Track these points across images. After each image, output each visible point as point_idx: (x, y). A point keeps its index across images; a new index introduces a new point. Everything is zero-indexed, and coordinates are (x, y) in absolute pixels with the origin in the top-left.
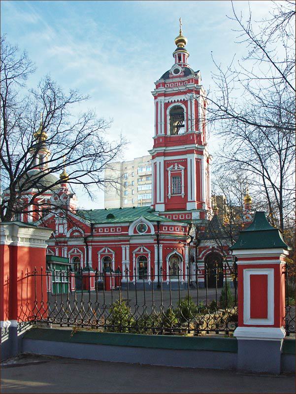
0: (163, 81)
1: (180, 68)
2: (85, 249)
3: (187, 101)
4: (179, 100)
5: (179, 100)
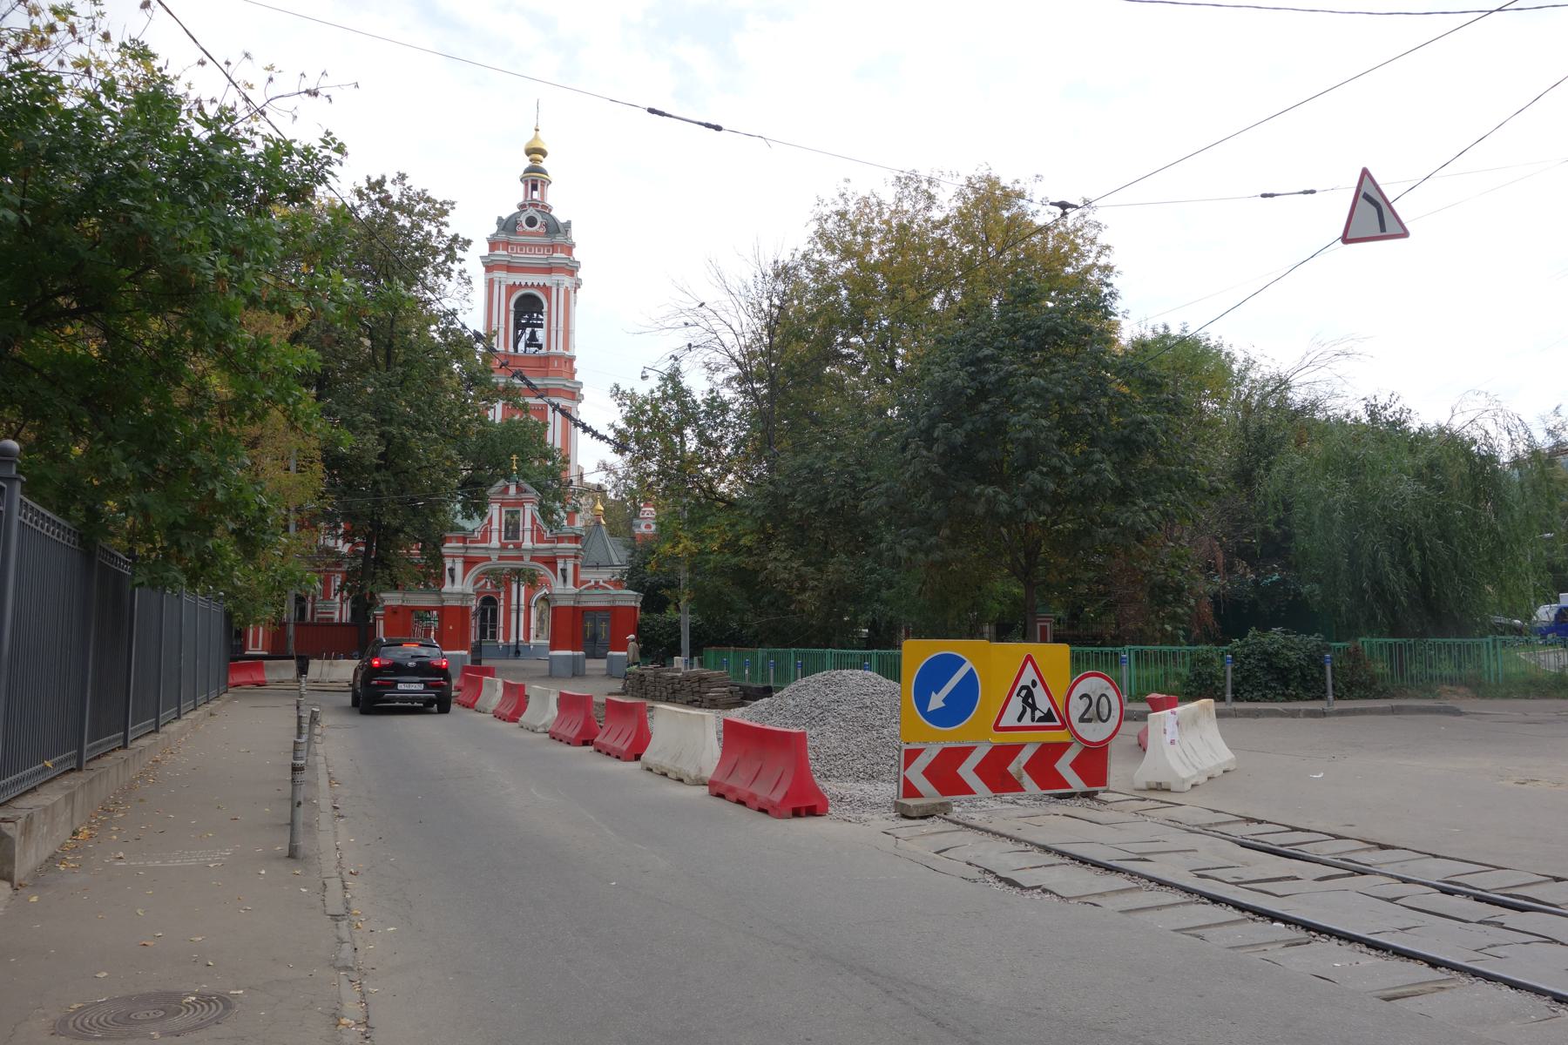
0: (503, 236)
1: (539, 219)
4: (536, 284)
5: (536, 284)
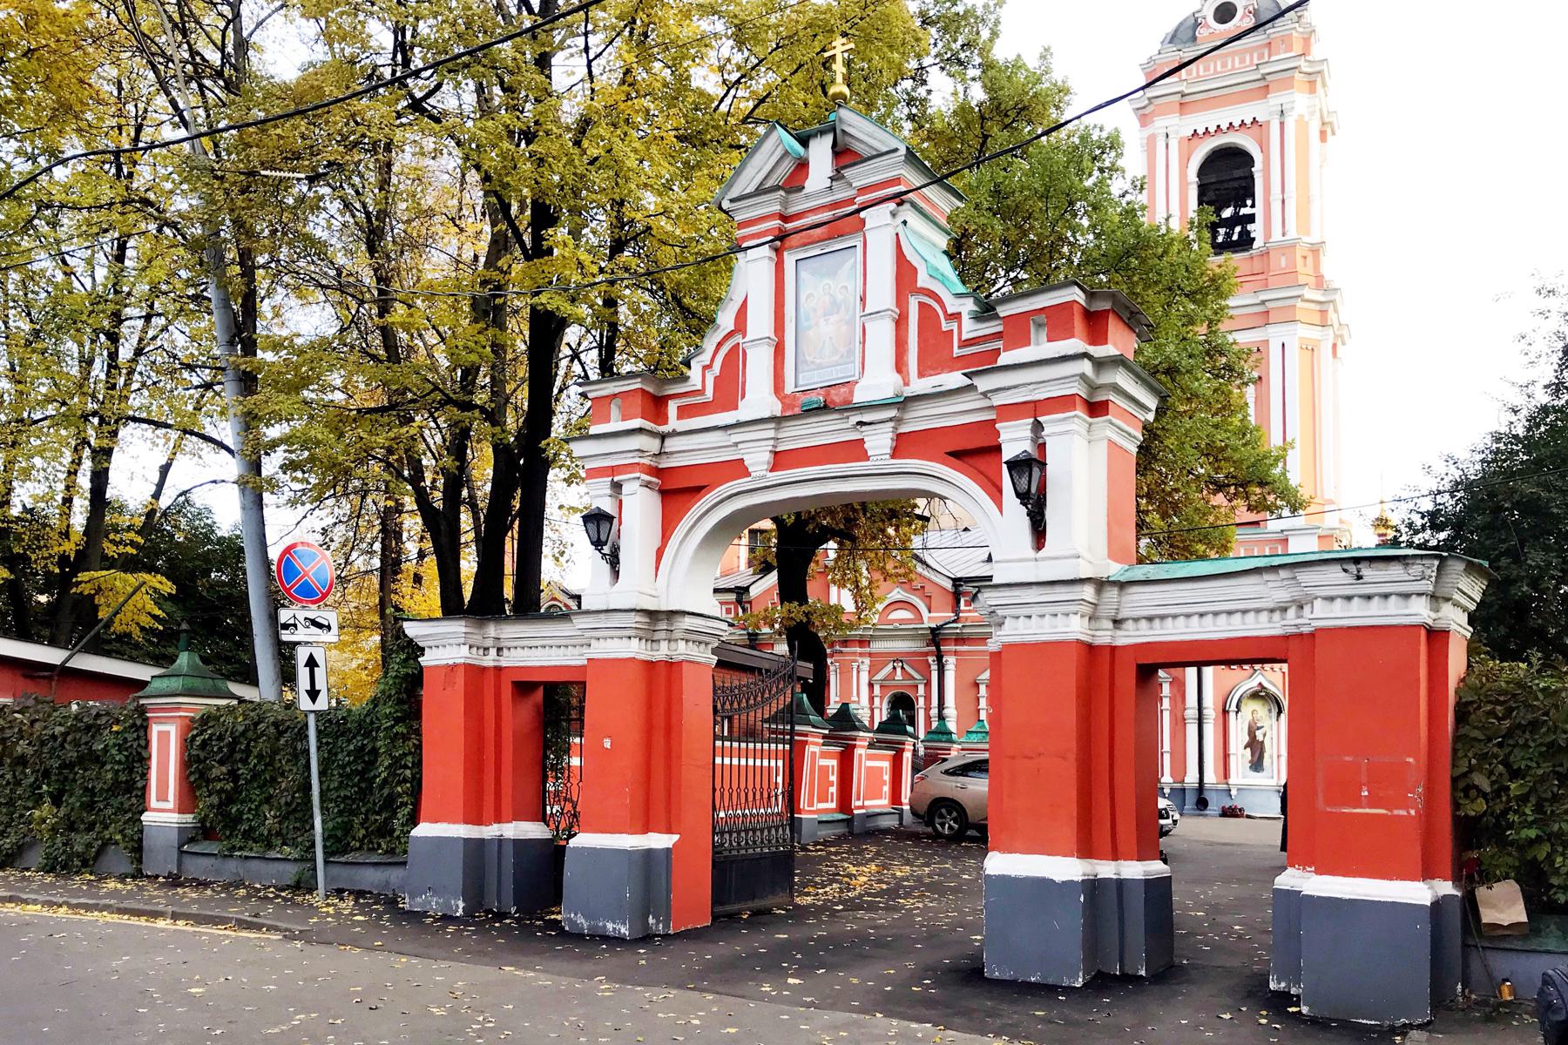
2: (934, 667)
3: (1268, 122)
